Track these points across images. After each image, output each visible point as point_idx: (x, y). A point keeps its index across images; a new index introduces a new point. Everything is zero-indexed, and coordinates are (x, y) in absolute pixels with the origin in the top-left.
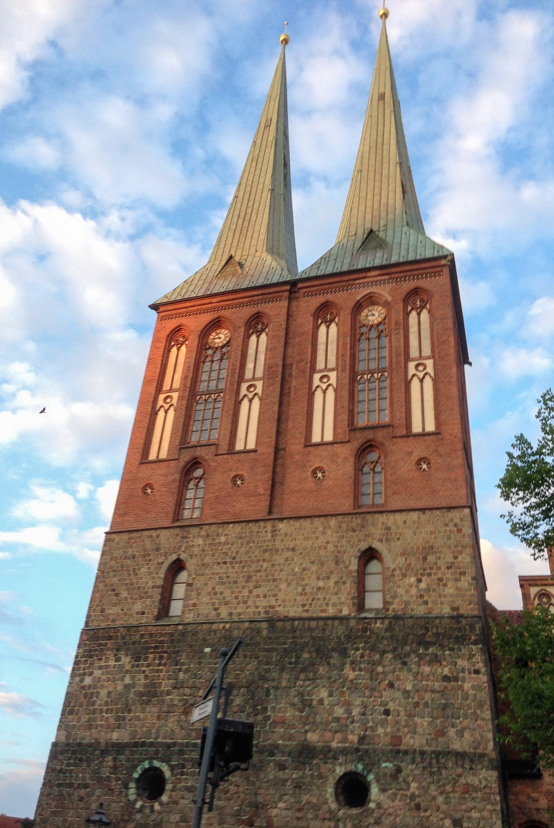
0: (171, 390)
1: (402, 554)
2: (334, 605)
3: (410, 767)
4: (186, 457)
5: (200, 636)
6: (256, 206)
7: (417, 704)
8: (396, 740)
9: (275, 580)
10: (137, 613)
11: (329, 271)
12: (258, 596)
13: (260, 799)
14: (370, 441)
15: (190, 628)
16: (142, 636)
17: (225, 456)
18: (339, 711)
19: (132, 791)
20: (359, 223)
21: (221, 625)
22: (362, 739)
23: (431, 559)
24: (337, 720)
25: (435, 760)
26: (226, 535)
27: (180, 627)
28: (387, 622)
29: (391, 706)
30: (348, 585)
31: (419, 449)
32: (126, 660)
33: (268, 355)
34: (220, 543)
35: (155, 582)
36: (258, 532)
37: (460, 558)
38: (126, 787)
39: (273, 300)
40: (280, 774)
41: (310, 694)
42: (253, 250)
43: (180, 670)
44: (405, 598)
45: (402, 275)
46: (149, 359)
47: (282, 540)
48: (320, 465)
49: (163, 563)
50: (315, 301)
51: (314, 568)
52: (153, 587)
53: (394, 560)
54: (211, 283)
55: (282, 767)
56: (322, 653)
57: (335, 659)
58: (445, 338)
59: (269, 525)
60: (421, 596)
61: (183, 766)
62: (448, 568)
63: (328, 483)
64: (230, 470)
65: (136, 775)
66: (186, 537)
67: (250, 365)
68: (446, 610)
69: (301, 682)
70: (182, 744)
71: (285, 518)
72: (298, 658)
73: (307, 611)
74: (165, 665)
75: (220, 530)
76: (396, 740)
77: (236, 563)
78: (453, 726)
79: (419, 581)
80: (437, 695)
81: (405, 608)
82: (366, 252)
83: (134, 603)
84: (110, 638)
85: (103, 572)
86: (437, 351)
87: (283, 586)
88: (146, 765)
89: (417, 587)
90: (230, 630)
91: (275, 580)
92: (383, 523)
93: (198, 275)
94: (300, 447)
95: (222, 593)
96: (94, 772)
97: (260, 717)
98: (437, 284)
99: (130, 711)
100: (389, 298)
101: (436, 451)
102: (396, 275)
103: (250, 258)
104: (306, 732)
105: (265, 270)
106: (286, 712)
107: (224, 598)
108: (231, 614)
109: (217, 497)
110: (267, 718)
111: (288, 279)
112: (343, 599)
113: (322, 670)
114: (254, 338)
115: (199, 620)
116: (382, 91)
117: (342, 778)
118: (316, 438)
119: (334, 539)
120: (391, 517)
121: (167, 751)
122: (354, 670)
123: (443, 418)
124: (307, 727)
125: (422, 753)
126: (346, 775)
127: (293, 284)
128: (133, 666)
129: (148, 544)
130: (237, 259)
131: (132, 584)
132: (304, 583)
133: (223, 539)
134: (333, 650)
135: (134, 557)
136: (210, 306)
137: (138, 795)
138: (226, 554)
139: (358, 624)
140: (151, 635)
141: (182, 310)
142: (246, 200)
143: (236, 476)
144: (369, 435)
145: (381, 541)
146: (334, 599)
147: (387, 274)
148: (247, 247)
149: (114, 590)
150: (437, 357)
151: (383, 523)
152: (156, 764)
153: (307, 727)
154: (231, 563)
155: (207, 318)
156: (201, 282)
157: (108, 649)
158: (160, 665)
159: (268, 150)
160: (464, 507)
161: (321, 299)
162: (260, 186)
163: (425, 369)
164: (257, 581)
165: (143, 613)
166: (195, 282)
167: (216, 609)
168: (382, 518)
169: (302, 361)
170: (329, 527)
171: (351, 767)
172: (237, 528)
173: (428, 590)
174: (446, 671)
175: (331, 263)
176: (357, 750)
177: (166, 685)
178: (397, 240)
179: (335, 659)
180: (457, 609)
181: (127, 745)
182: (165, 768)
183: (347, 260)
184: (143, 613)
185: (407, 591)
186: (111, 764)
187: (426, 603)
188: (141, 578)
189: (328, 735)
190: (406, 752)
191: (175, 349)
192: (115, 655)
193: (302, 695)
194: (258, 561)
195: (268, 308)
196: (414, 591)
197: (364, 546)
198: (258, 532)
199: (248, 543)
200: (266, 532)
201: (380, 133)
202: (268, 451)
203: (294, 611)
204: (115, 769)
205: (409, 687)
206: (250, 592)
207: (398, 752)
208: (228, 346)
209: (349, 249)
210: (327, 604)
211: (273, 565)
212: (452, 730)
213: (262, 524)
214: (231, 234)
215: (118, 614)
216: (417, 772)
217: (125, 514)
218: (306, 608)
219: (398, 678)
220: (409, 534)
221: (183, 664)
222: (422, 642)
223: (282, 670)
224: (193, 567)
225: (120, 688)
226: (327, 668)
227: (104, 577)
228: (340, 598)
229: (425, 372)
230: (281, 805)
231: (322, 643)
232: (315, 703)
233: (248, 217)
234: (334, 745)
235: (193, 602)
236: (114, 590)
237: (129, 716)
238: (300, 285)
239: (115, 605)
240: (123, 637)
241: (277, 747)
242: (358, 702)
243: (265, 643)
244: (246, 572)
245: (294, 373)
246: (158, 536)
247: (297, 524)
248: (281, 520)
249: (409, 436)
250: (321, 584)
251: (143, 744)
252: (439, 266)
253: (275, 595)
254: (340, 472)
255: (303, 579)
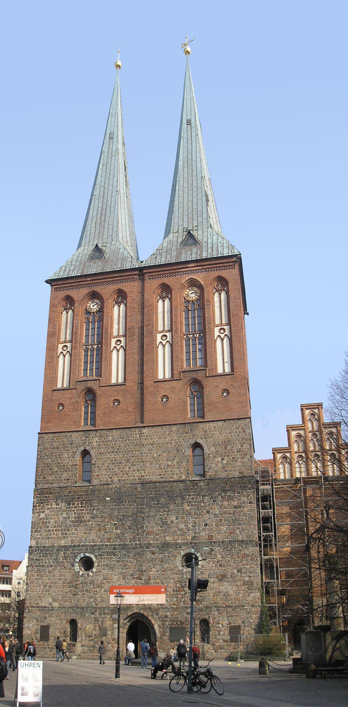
0: (65, 342)
1: (213, 446)
2: (177, 474)
3: (217, 549)
4: (81, 387)
5: (103, 492)
6: (109, 203)
7: (221, 520)
8: (210, 537)
9: (143, 462)
10: (65, 480)
11: (163, 261)
12: (134, 471)
13: (144, 568)
14: (194, 379)
15: (97, 487)
16: (70, 492)
17: (107, 387)
18: (182, 526)
19: (77, 567)
20: (180, 224)
21: (114, 486)
22: (194, 538)
23: (229, 447)
24: (182, 530)
25: (229, 545)
26: (112, 436)
27: (91, 487)
28: (206, 481)
29: (208, 522)
30: (184, 464)
31: (222, 384)
32: (63, 505)
33: (128, 320)
34: (108, 441)
35: (73, 463)
36: (131, 434)
37: (244, 447)
38: (73, 565)
39: (127, 280)
40: (153, 556)
41: (165, 519)
42: (110, 239)
43: (93, 509)
44: (215, 469)
45: (209, 267)
46: (50, 319)
47: (145, 439)
48: (165, 394)
49: (76, 452)
50: (155, 283)
51: (165, 454)
52: (72, 465)
53: (209, 450)
54: (85, 264)
55: (153, 553)
56: (171, 498)
57: (179, 501)
58: (236, 312)
59: (137, 430)
60: (224, 468)
61: (102, 555)
62: (238, 452)
63: (171, 404)
64: (110, 396)
65: (77, 560)
66: (88, 437)
67: (115, 326)
68: (237, 474)
69: (161, 513)
70: (99, 545)
71: (146, 426)
72: (158, 501)
73: (163, 478)
74: (85, 507)
75: (108, 433)
76: (210, 537)
77: (120, 452)
78: (239, 529)
79: (223, 459)
80: (231, 515)
81: (216, 474)
82: (185, 247)
83: (62, 474)
84: (51, 493)
85: (41, 456)
86: (232, 320)
87: (148, 465)
88: (82, 555)
89: (222, 462)
90: (119, 488)
91: (143, 462)
92: (203, 429)
93: (75, 257)
94: (152, 383)
95: (113, 469)
96: (55, 559)
97: (140, 531)
98: (230, 274)
99: (68, 530)
100: (202, 283)
101: (231, 385)
102: (206, 267)
103: (108, 245)
104: (165, 536)
105: (120, 257)
106: (153, 528)
107: (115, 472)
108: (119, 480)
109: (104, 413)
110: (144, 531)
111: (137, 267)
112: (182, 471)
113: (172, 507)
114: (116, 307)
115: (102, 483)
116: (189, 117)
117: (183, 556)
118: (161, 377)
119: (175, 437)
120: (207, 424)
121: (92, 548)
122: (189, 506)
123: (235, 364)
124: (165, 534)
125: (223, 542)
126: (187, 554)
127: (141, 269)
128: (67, 508)
129: (65, 440)
130: (99, 245)
131: (59, 463)
132: (160, 463)
133: (110, 438)
134: (177, 497)
135: (58, 448)
136: (86, 283)
137: (80, 569)
138: (113, 447)
139: (191, 483)
140: (75, 492)
141: (67, 285)
142: (101, 198)
143: (115, 400)
144: (194, 375)
145: (201, 438)
146: (177, 471)
147: (200, 266)
148: (105, 237)
149: (49, 467)
150: (232, 325)
151: (203, 429)
152: (87, 555)
153: (165, 534)
154: (116, 452)
155: (85, 291)
156: (77, 264)
157: (51, 499)
158: (82, 507)
159: (113, 158)
160: (247, 418)
161: (160, 281)
162: (110, 187)
163: (224, 332)
164: (133, 462)
165: (68, 480)
166: (74, 263)
167: (110, 478)
168: (202, 426)
169: (150, 325)
170: (172, 431)
171: (187, 551)
172: (119, 432)
173: (227, 464)
174: (236, 503)
175: (164, 255)
176: (191, 543)
177: (87, 517)
178: (205, 239)
179: (179, 501)
180: (242, 473)
181: (70, 546)
182: (92, 556)
183: (174, 254)
184: (68, 480)
185: (217, 465)
186: (63, 556)
187: (226, 471)
188: (64, 460)
189: (176, 537)
190: (214, 542)
191: (64, 313)
192: (56, 502)
193: (161, 519)
194: (132, 451)
195: (126, 286)
196: (220, 465)
197: (192, 441)
198: (131, 434)
199: (125, 441)
200: (136, 434)
201: (190, 151)
202: (133, 384)
203: (155, 478)
204: (65, 558)
205: (218, 513)
206: (130, 468)
207: (211, 543)
208: (100, 312)
209: (175, 244)
210: (173, 474)
211: (142, 454)
212: (238, 530)
213: (133, 430)
214: (94, 225)
215: (53, 480)
216: (220, 550)
217: (47, 422)
218: (162, 476)
219: (211, 508)
220: (217, 434)
221: (94, 506)
222: (224, 491)
223: (151, 507)
224: (94, 454)
225: (61, 519)
226: (175, 505)
227: (41, 459)
228: (180, 471)
229: (225, 334)
230: (154, 569)
231: (171, 493)
232: (169, 522)
233: (104, 212)
234: (179, 541)
235: (97, 474)
236: (49, 467)
237: (68, 533)
238: (145, 271)
239: (51, 475)
240: (58, 493)
241: (150, 544)
242: (191, 520)
243: (139, 495)
244: (126, 457)
245: (145, 334)
246: (71, 436)
247: (154, 429)
248: (144, 427)
249: (217, 376)
250: (170, 463)
251: (79, 546)
252: (232, 262)
253: (144, 470)
254: (177, 398)
255: (159, 461)
